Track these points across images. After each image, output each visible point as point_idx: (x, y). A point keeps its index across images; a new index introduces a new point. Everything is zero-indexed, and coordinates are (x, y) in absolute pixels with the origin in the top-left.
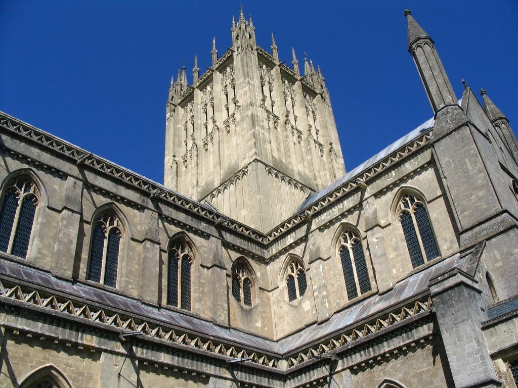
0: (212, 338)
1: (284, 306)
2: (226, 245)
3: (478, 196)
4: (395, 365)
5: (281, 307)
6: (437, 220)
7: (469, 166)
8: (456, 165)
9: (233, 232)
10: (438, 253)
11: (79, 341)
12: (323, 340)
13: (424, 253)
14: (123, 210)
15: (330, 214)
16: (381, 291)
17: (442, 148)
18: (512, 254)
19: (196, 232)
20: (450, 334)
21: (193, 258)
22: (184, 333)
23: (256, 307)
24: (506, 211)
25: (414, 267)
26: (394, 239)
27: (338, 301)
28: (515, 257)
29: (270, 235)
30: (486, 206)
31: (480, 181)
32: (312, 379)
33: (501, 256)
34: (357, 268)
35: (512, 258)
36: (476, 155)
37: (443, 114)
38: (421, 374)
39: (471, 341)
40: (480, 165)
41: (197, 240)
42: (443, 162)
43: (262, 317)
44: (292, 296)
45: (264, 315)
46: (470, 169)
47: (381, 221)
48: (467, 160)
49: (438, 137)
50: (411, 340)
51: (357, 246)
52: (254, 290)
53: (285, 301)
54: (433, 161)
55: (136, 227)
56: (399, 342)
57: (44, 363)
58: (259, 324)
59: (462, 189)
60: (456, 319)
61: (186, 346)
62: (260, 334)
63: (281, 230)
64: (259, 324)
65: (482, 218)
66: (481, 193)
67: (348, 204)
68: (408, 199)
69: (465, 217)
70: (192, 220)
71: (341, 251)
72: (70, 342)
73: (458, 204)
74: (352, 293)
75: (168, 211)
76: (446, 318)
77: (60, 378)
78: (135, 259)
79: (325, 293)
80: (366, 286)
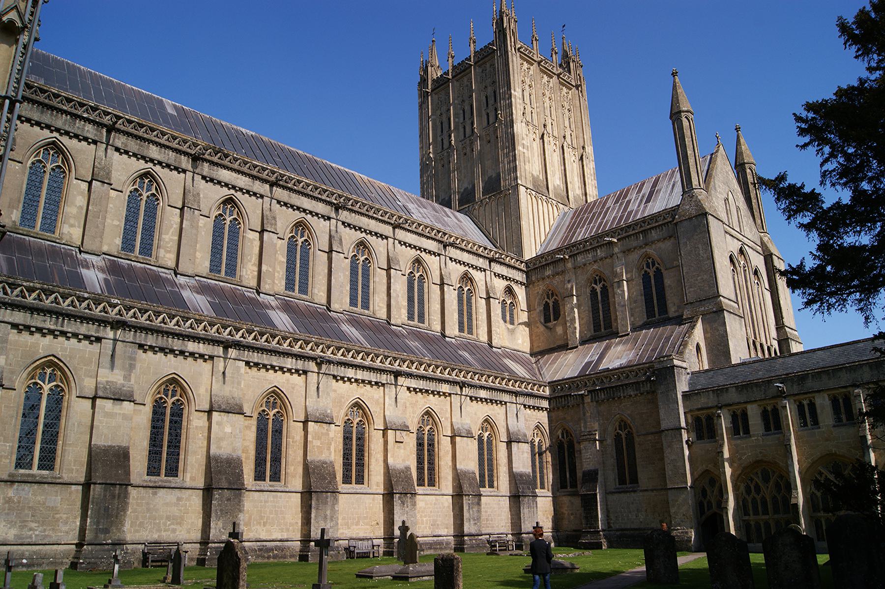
5: (538, 327)
6: (670, 286)
7: (701, 252)
10: (666, 312)
13: (656, 309)
17: (682, 230)
18: (718, 330)
25: (648, 319)
26: (635, 293)
42: (682, 242)
44: (547, 320)
48: (700, 246)
51: (604, 290)
55: (435, 272)
58: (520, 341)
62: (520, 349)
64: (520, 341)
66: (705, 277)
68: (650, 261)
75: (456, 254)
77: (433, 413)
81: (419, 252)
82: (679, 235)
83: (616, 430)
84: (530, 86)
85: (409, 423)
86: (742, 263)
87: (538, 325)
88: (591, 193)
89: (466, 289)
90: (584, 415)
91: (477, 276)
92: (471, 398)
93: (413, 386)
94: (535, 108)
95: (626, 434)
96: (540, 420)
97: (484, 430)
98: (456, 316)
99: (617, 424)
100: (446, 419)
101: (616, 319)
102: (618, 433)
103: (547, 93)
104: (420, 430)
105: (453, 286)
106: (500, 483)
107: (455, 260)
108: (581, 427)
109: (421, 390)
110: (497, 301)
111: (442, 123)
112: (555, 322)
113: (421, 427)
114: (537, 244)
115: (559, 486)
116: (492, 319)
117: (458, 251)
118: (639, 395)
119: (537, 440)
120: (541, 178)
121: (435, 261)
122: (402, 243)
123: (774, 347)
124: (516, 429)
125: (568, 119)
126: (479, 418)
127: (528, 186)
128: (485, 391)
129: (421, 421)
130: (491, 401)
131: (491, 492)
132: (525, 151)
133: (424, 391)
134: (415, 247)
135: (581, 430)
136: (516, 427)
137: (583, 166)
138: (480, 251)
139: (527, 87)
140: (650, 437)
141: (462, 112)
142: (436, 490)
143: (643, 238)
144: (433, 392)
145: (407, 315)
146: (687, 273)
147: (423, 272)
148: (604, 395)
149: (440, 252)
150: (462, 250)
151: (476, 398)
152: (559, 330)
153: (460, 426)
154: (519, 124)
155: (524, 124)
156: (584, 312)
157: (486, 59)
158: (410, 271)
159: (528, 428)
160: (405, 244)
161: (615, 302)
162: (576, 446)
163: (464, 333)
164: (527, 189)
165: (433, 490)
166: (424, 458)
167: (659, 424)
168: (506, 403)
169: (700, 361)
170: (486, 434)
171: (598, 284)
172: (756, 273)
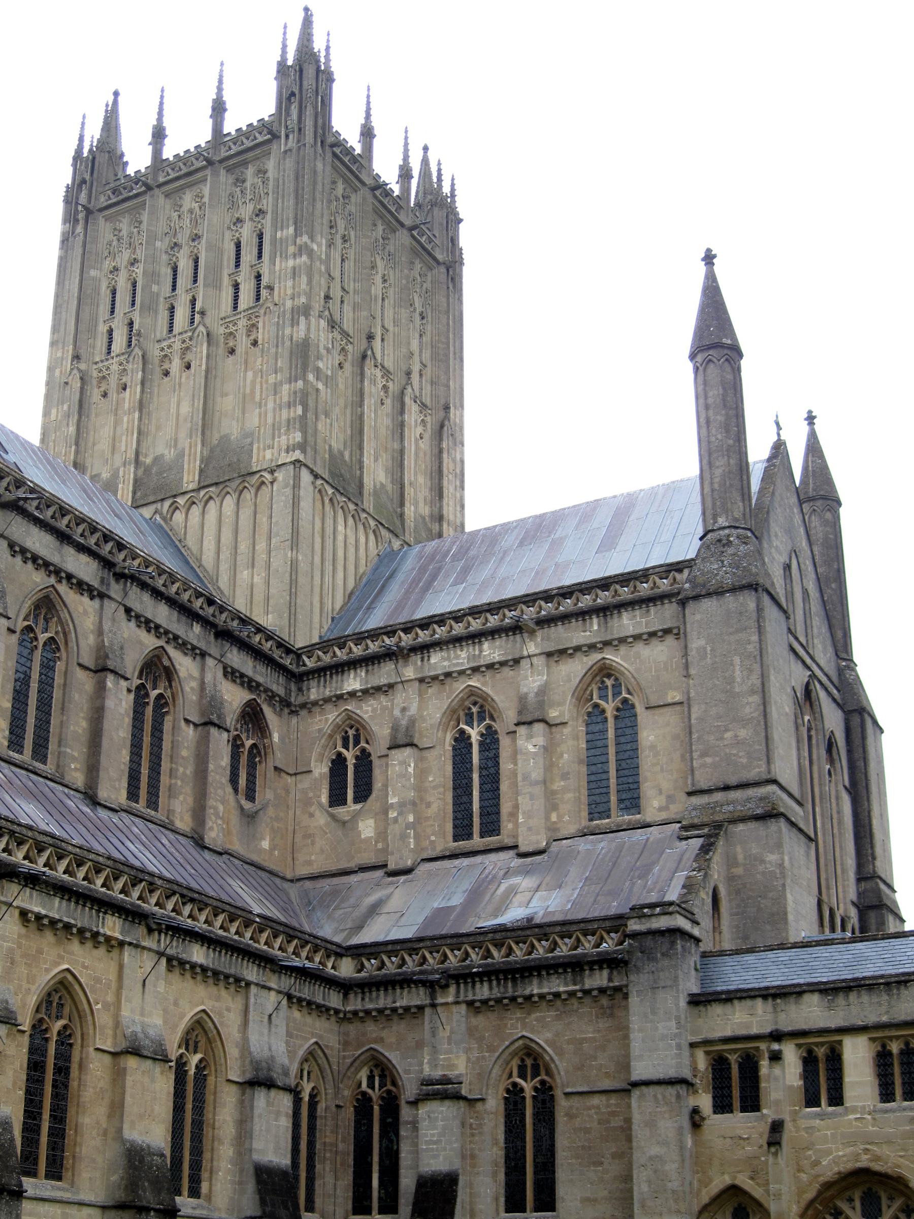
0: (258, 920)
1: (318, 813)
2: (231, 674)
3: (736, 736)
4: (544, 1017)
5: (311, 815)
6: (653, 747)
7: (738, 673)
8: (716, 662)
9: (244, 646)
11: (101, 931)
12: (428, 943)
14: (68, 601)
15: (448, 659)
16: (523, 848)
18: (763, 861)
19: (184, 646)
20: (642, 1000)
21: (170, 701)
22: (224, 911)
23: (264, 808)
24: (775, 782)
27: (433, 838)
28: (766, 868)
29: (310, 650)
30: (744, 761)
31: (747, 710)
32: (398, 1004)
33: (745, 858)
34: (481, 785)
35: (761, 868)
36: (755, 657)
37: (720, 541)
38: (582, 1041)
39: (670, 1019)
40: (755, 680)
41: (184, 665)
43: (272, 829)
44: (337, 798)
45: (276, 825)
46: (739, 680)
47: (550, 711)
48: (737, 660)
49: (698, 590)
50: (577, 987)
51: (490, 741)
52: (264, 770)
53: (320, 805)
54: (675, 631)
55: (87, 638)
56: (558, 985)
57: (59, 964)
58: (265, 844)
59: (713, 712)
60: (655, 982)
61: (225, 934)
63: (334, 653)
64: (265, 844)
65: (733, 781)
66: (743, 733)
67: (491, 651)
69: (704, 765)
70: (178, 621)
71: (456, 740)
72: (91, 931)
73: (699, 738)
74: (462, 830)
76: (641, 975)
77: (77, 987)
78: (82, 709)
79: (411, 818)
80: (491, 826)
81: (52, 580)
82: (688, 630)
83: (510, 1076)
84: (345, 239)
85: (15, 1003)
86: (807, 718)
87: (312, 809)
88: (451, 517)
89: (154, 694)
90: (434, 1034)
91: (184, 665)
92: (170, 960)
93: (36, 909)
94: (351, 293)
95: (536, 1089)
96: (320, 1037)
97: (191, 1048)
98: (125, 756)
99: (515, 1063)
100: (106, 1006)
101: (513, 815)
102: (515, 1085)
103: (380, 264)
104: (39, 1029)
105: (127, 679)
106: (218, 1187)
107: (138, 617)
108: (421, 1064)
109: (53, 922)
110: (225, 735)
111: (114, 293)
112: (358, 806)
113: (41, 1021)
114: (325, 615)
115: (350, 1207)
116: (210, 779)
117: (146, 597)
118: (579, 994)
119: (307, 1088)
120: (347, 457)
121: (90, 610)
122: (17, 549)
123: (852, 921)
124: (266, 1054)
125: (417, 336)
126: (182, 1016)
127: (320, 471)
128: (205, 948)
129: (44, 1005)
130: (216, 973)
131: (194, 1208)
132: (320, 386)
133: (60, 925)
134: (46, 564)
135: (422, 1071)
136: (266, 1048)
137: (441, 451)
138: (198, 603)
139: (339, 241)
140: (596, 1100)
141: (169, 271)
142: (67, 1190)
143: (599, 625)
144: (81, 931)
145: (7, 733)
146: (701, 719)
147: (57, 633)
148: (491, 988)
149: (103, 589)
150: (157, 594)
151: (182, 963)
152: (367, 828)
153: (138, 1029)
154: (313, 320)
155: (323, 323)
156: (435, 788)
157: (250, 155)
158: (26, 623)
159: (291, 1053)
160: (23, 551)
161: (514, 774)
162: (406, 1113)
163: (137, 802)
164: (316, 476)
165: (59, 1189)
166: (41, 1102)
167: (626, 1066)
168: (248, 984)
169: (716, 929)
170: (195, 1059)
171: (475, 724)
172: (830, 745)
